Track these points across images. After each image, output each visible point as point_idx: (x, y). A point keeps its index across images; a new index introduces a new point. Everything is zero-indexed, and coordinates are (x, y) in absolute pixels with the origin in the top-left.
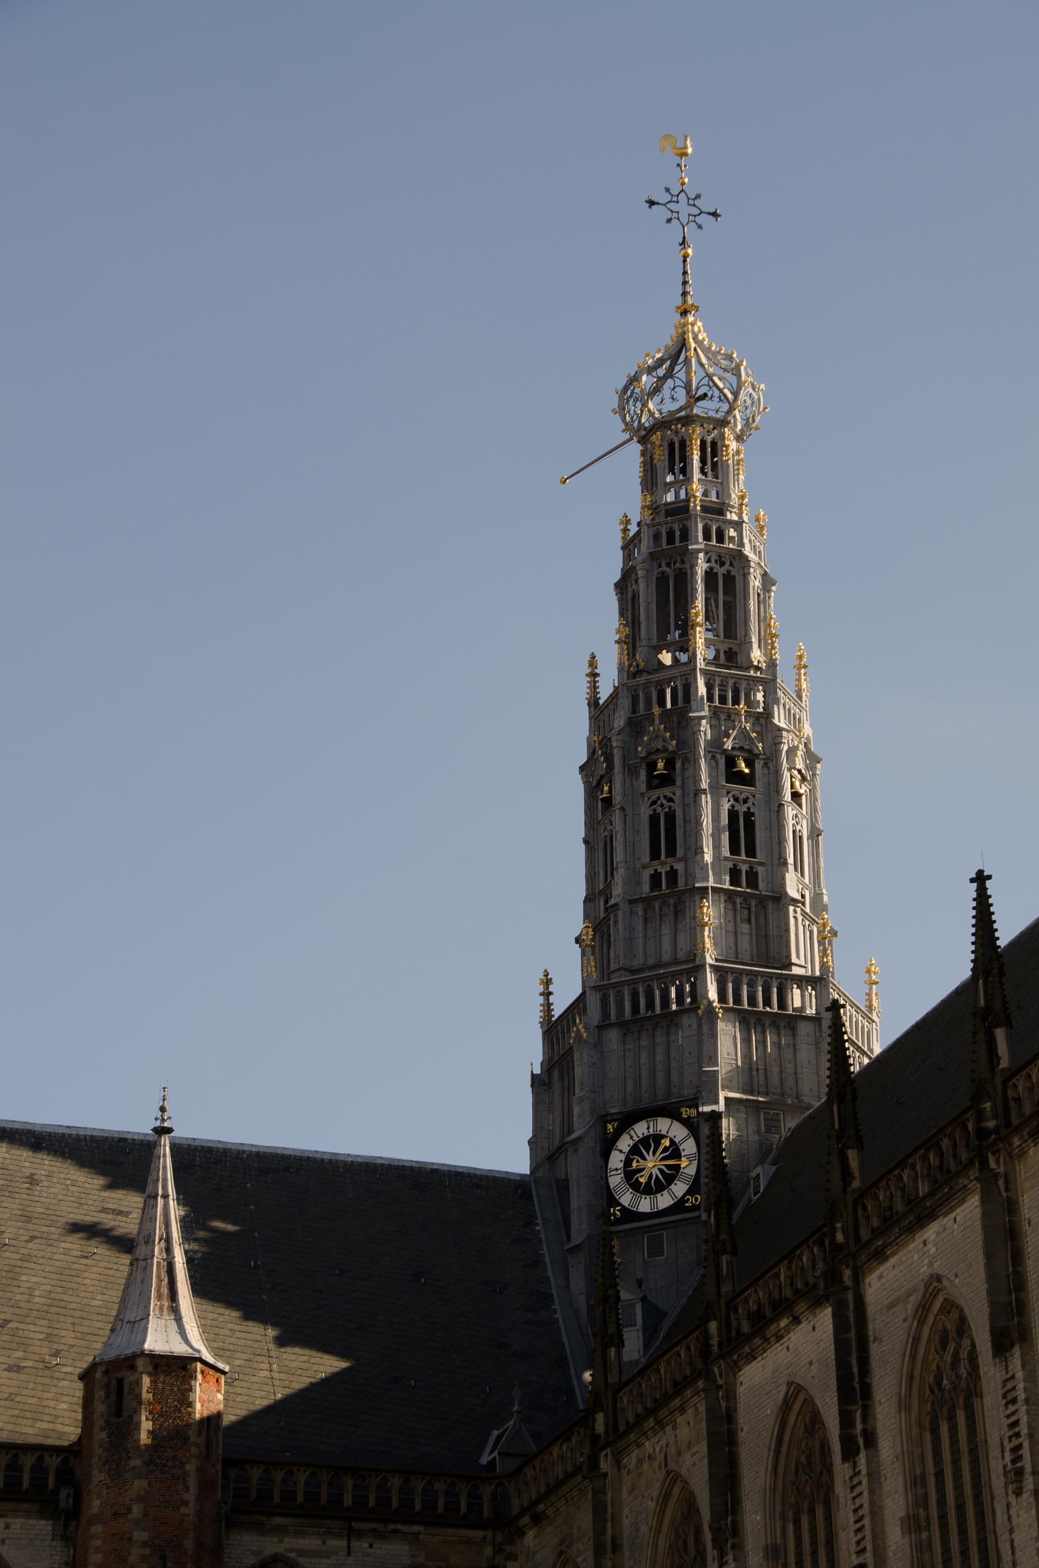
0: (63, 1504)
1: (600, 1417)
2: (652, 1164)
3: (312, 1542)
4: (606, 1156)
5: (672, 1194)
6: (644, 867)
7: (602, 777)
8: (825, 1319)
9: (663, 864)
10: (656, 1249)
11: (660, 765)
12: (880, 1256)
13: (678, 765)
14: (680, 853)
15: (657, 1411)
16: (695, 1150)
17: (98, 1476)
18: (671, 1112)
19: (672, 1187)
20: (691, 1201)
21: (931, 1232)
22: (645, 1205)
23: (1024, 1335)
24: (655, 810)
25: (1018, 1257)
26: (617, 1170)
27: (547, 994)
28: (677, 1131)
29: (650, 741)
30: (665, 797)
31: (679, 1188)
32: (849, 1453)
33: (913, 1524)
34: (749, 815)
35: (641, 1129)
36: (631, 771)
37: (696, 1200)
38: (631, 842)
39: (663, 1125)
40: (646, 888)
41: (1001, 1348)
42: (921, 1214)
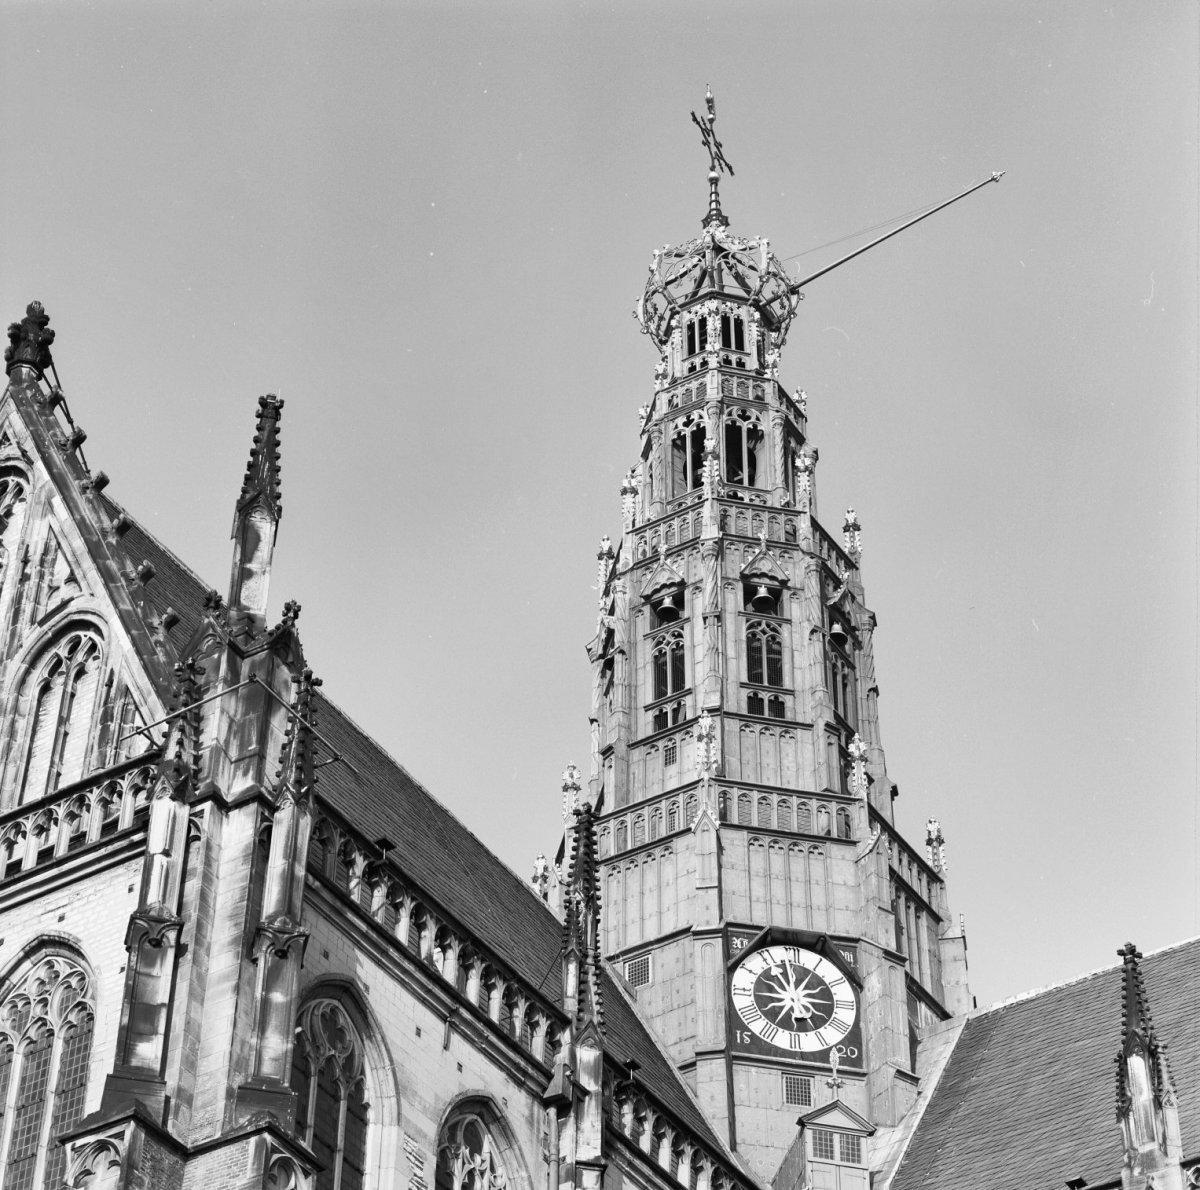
2: (795, 1000)
4: (731, 970)
5: (821, 1039)
6: (743, 685)
7: (664, 586)
9: (764, 689)
14: (787, 684)
16: (853, 999)
18: (820, 944)
19: (821, 1030)
24: (754, 635)
26: (744, 989)
28: (828, 971)
29: (753, 562)
30: (768, 625)
35: (779, 953)
37: (853, 1052)
39: (809, 959)
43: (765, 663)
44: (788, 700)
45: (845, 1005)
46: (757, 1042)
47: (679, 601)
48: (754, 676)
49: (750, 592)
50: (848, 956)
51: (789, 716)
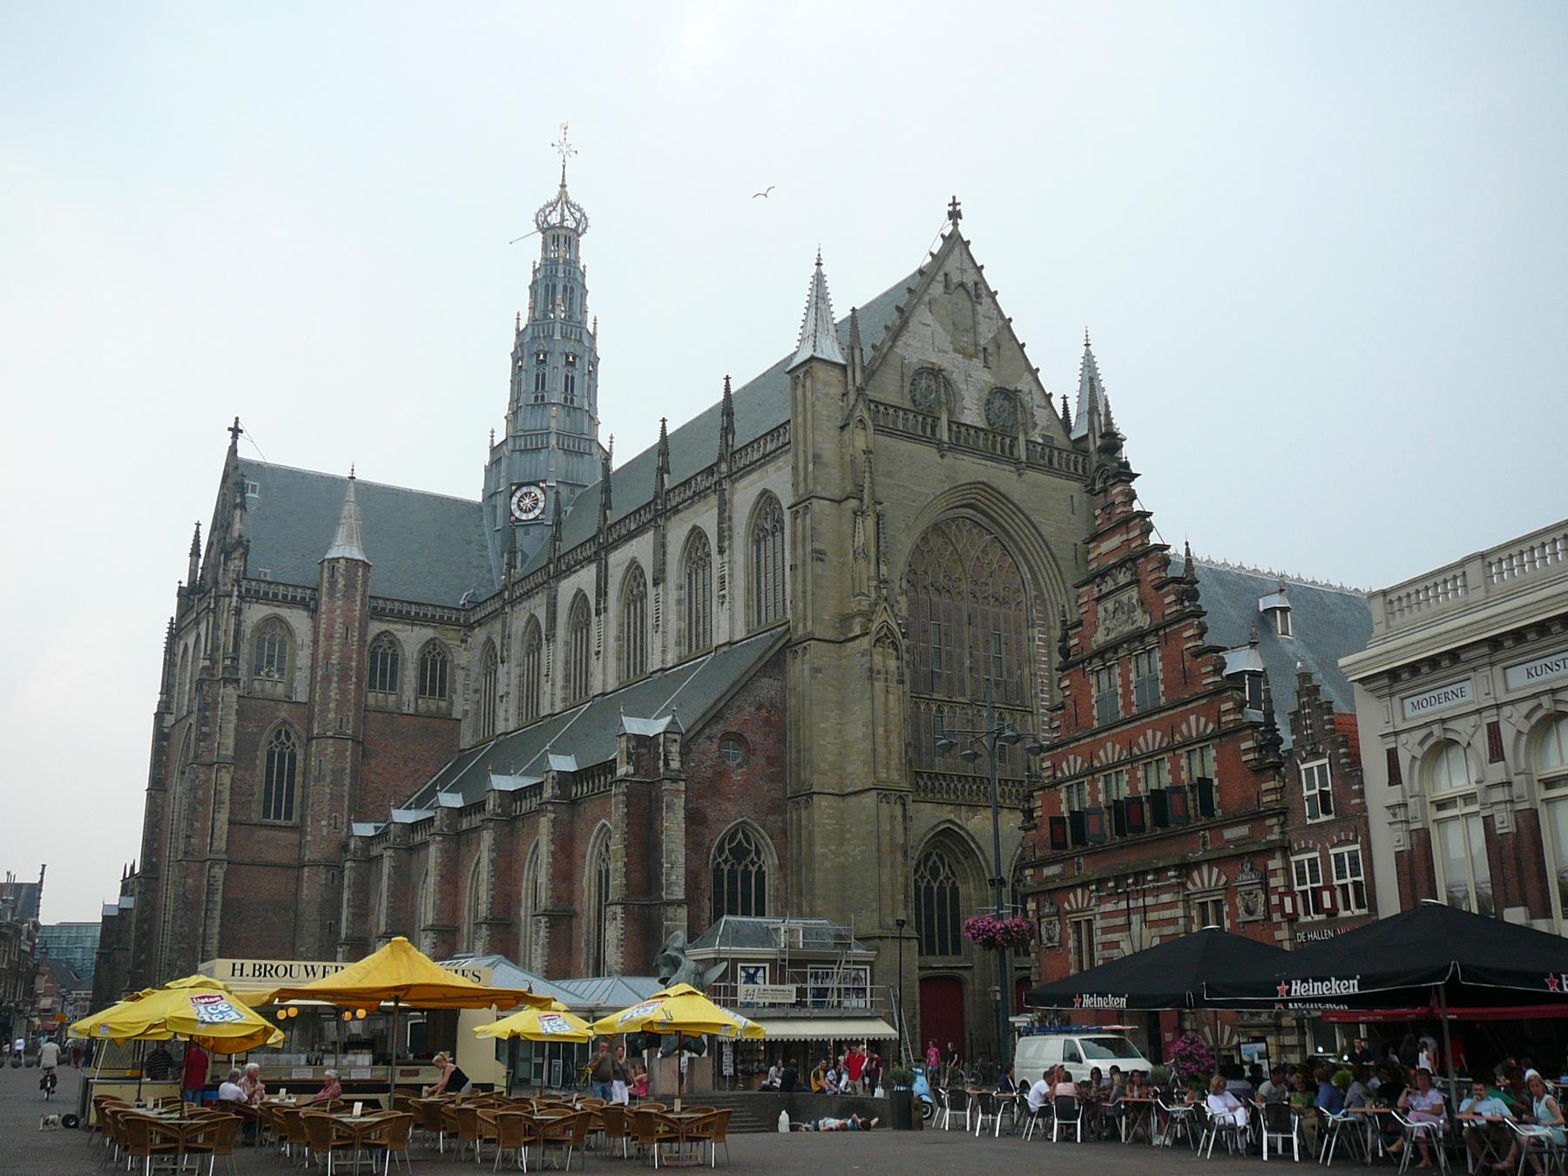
3: (399, 626)
8: (593, 568)
10: (527, 533)
12: (615, 548)
15: (528, 595)
17: (325, 598)
18: (536, 484)
21: (634, 542)
22: (524, 517)
23: (664, 581)
25: (664, 554)
28: (538, 492)
31: (537, 512)
32: (598, 614)
33: (618, 638)
35: (525, 490)
38: (529, 385)
39: (533, 489)
41: (656, 584)
42: (631, 535)
43: (541, 382)
46: (518, 520)
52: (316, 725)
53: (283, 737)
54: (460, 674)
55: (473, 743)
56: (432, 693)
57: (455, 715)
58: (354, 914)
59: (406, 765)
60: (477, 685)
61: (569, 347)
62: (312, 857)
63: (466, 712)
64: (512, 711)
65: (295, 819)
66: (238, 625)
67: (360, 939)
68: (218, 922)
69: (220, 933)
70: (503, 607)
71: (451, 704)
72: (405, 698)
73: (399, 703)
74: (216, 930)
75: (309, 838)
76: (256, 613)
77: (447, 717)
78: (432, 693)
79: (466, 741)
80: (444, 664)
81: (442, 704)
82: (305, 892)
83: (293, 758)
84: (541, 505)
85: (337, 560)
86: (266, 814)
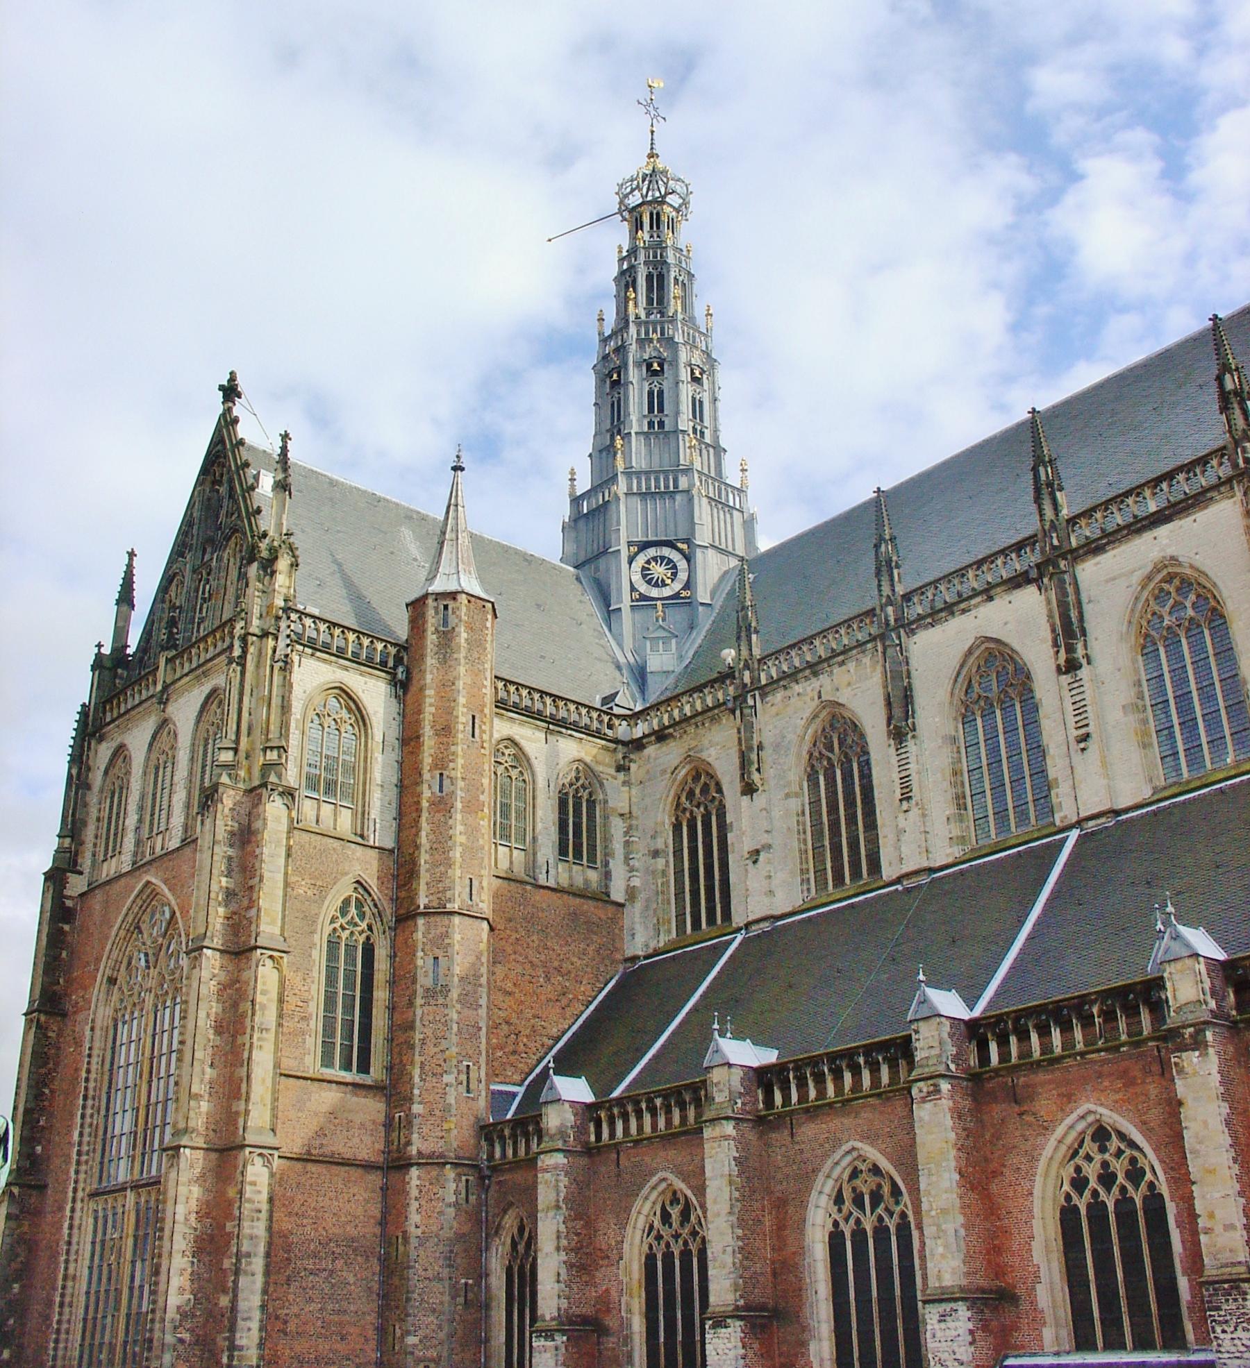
0: (400, 676)
1: (747, 673)
2: (659, 571)
4: (630, 563)
5: (672, 589)
11: (656, 366)
13: (666, 367)
17: (430, 661)
18: (670, 544)
20: (684, 594)
22: (654, 593)
27: (572, 480)
34: (701, 402)
35: (652, 552)
36: (638, 364)
39: (666, 552)
40: (646, 429)
44: (667, 421)
45: (683, 570)
46: (643, 597)
47: (619, 376)
48: (651, 410)
49: (649, 366)
50: (684, 547)
51: (666, 429)
52: (423, 888)
53: (353, 911)
54: (617, 827)
55: (653, 944)
56: (578, 854)
57: (618, 895)
58: (570, 1266)
59: (548, 979)
60: (660, 844)
61: (697, 359)
62: (427, 1147)
63: (631, 893)
64: (780, 877)
65: (377, 1071)
66: (287, 685)
67: (585, 1320)
68: (259, 1280)
69: (263, 1307)
70: (740, 698)
71: (607, 875)
72: (541, 859)
73: (531, 866)
74: (256, 1300)
75: (417, 1108)
76: (312, 675)
77: (602, 897)
78: (578, 854)
79: (641, 936)
80: (592, 804)
81: (593, 876)
82: (415, 1218)
83: (369, 950)
84: (683, 576)
85: (453, 595)
86: (327, 1061)
